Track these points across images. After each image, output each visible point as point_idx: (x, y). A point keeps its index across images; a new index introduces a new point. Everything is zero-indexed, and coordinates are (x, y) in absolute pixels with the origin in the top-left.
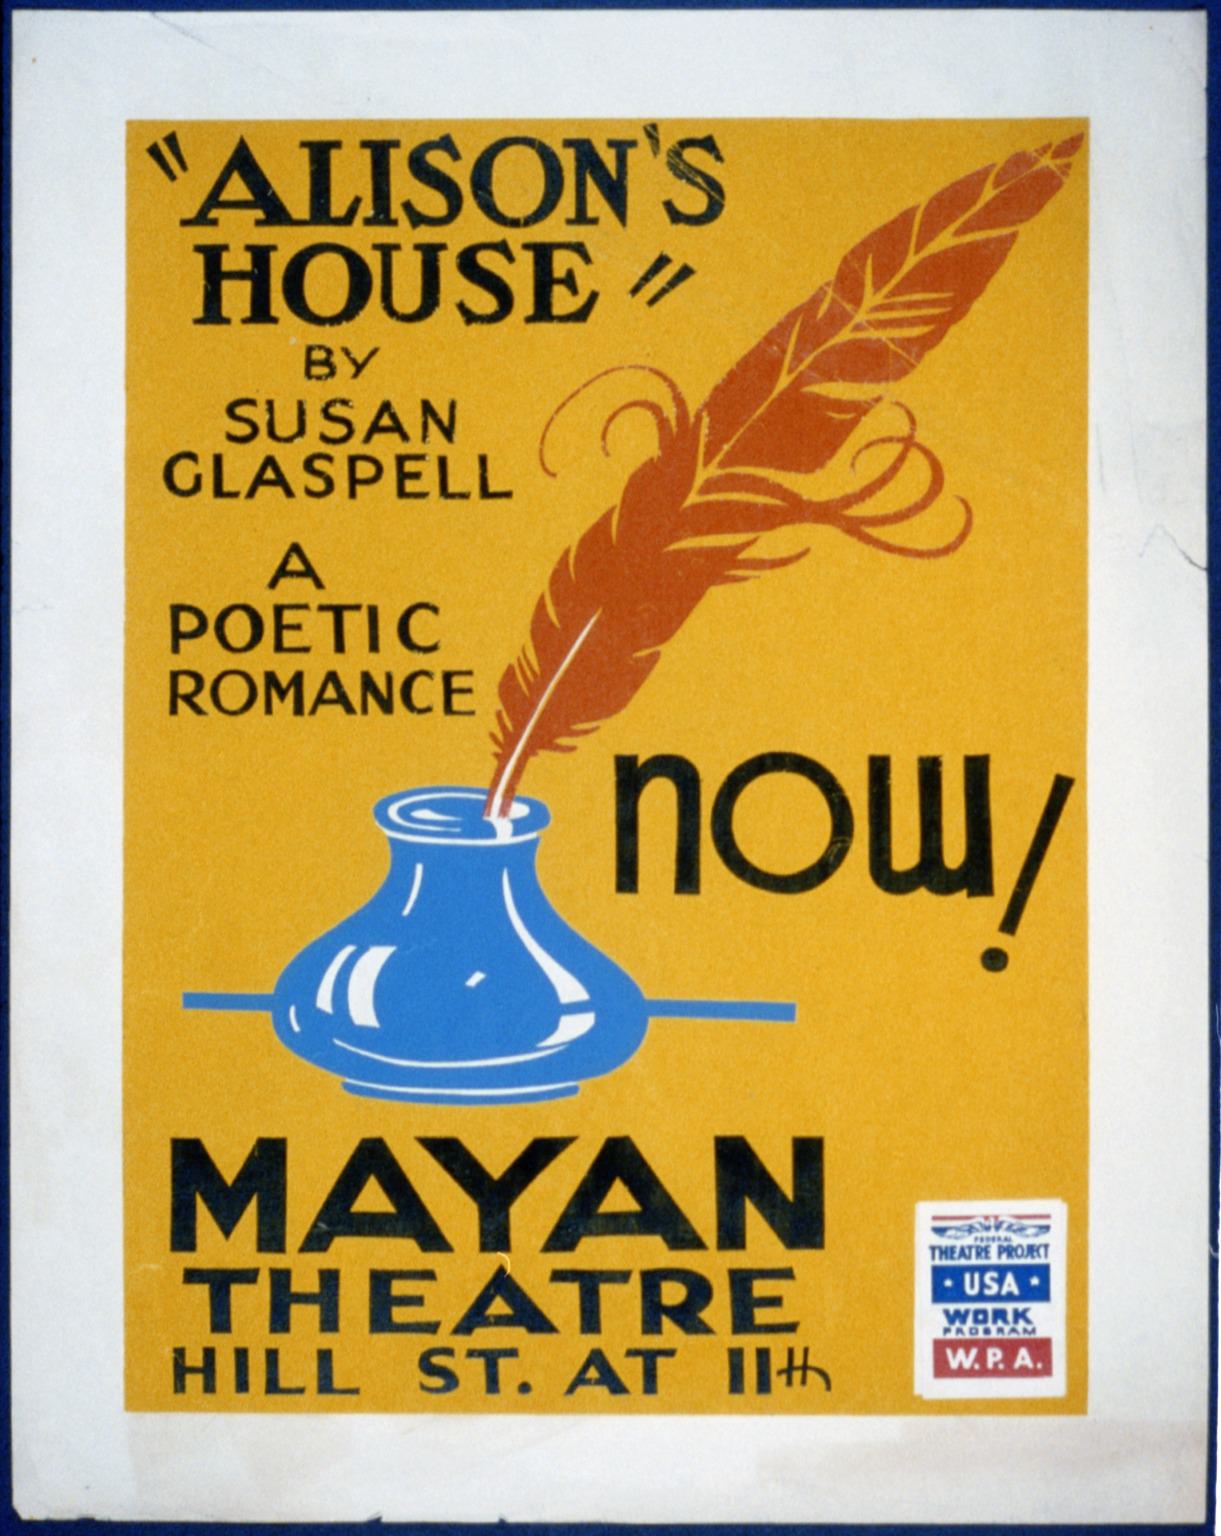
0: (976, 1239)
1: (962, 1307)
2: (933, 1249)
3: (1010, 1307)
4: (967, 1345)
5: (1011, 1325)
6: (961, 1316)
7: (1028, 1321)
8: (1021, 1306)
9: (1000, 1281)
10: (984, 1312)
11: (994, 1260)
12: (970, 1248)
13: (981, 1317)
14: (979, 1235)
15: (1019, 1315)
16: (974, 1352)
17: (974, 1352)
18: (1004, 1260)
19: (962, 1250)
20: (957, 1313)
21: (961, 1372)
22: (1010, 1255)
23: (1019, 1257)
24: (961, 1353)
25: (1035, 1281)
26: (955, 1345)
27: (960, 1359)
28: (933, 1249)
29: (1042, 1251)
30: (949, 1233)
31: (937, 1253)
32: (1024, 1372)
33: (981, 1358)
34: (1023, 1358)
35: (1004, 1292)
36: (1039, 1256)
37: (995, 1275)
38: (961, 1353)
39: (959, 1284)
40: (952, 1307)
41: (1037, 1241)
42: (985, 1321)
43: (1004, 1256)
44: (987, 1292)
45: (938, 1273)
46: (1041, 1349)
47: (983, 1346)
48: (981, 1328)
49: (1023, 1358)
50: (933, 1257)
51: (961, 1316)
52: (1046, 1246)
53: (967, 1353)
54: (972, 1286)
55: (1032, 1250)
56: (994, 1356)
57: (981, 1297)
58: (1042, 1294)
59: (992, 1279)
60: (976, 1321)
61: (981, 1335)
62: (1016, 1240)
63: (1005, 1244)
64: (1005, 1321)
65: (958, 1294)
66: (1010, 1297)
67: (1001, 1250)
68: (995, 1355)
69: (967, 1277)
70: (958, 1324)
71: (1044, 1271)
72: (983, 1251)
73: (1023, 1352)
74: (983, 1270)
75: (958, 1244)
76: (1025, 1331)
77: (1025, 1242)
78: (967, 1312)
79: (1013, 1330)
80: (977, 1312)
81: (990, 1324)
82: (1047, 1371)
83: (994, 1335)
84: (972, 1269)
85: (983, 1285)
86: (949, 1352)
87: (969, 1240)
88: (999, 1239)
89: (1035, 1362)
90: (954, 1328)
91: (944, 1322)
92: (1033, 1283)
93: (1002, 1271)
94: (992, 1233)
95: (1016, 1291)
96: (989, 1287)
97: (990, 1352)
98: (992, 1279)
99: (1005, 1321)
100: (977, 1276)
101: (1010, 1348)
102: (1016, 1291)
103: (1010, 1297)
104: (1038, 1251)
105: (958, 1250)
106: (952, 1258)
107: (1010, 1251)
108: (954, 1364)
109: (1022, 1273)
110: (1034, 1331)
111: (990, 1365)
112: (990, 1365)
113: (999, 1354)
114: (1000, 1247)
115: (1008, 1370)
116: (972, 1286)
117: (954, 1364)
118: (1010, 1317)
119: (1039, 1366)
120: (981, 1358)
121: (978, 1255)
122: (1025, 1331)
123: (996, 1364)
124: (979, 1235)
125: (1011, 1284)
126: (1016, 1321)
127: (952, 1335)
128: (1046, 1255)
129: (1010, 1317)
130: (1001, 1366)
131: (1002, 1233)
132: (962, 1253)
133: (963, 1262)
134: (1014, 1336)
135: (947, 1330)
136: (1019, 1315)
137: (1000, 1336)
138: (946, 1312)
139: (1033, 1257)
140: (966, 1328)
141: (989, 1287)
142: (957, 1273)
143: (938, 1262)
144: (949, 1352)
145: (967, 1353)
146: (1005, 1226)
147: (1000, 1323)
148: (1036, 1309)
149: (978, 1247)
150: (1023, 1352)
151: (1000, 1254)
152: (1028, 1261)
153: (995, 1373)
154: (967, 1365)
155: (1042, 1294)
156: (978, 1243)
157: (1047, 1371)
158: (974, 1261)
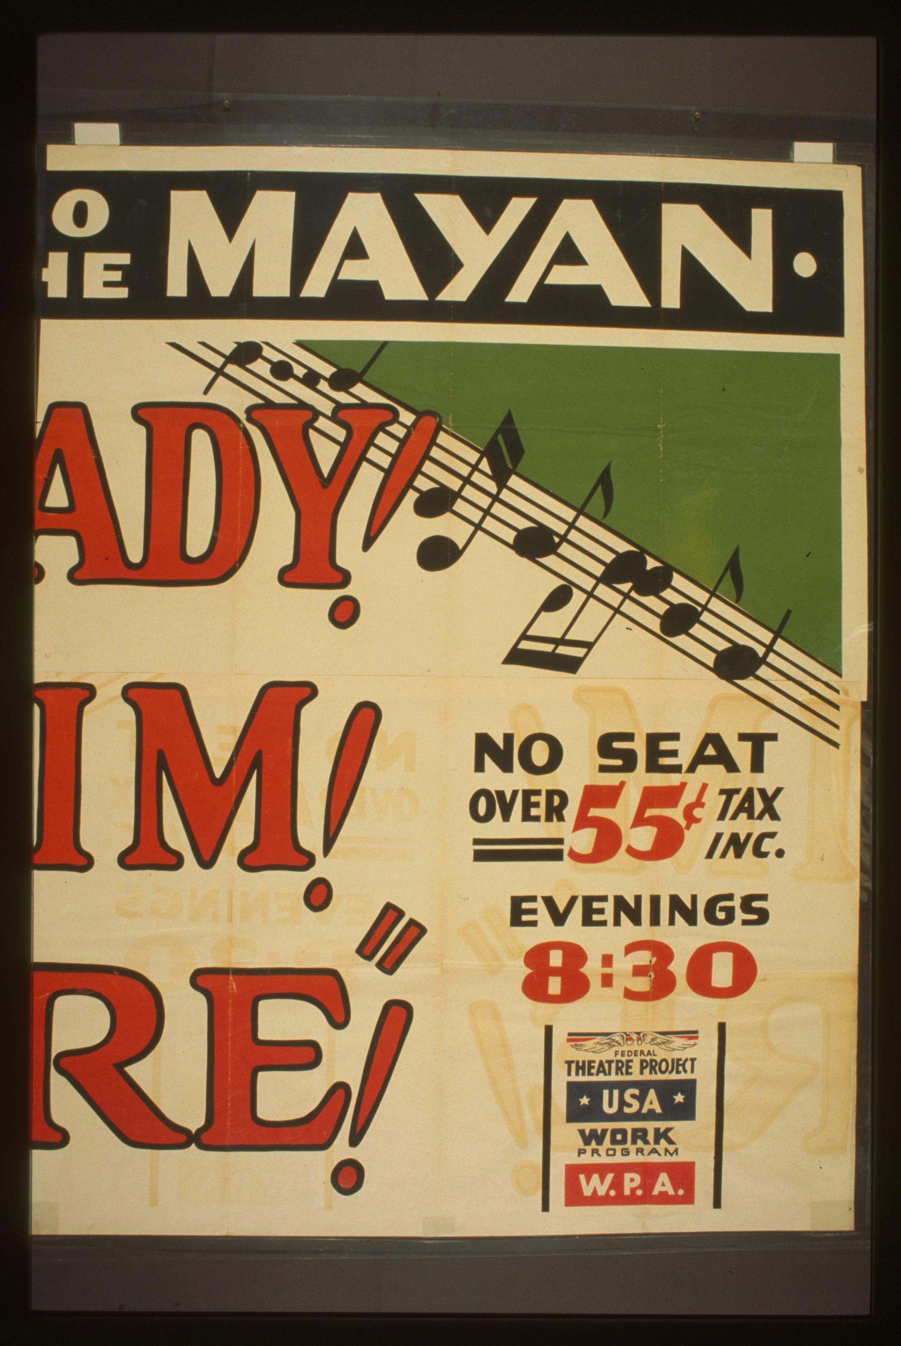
0: (616, 1053)
1: (599, 1126)
2: (569, 1063)
3: (650, 1126)
4: (602, 1170)
5: (652, 1146)
6: (598, 1137)
7: (671, 1142)
8: (662, 1125)
9: (641, 1099)
10: (624, 1132)
11: (636, 1076)
12: (610, 1062)
13: (619, 1137)
14: (620, 1049)
15: (660, 1135)
16: (610, 1177)
17: (610, 1177)
18: (647, 1076)
19: (601, 1064)
20: (593, 1132)
21: (595, 1200)
22: (653, 1070)
23: (662, 1072)
24: (595, 1177)
25: (679, 1098)
26: (589, 1170)
27: (593, 1185)
28: (569, 1063)
29: (688, 1065)
30: (589, 1044)
31: (573, 1066)
32: (664, 1199)
33: (617, 1184)
34: (663, 1184)
35: (644, 1110)
36: (685, 1071)
37: (636, 1092)
38: (595, 1177)
39: (597, 1100)
40: (588, 1127)
41: (683, 1055)
42: (624, 1141)
43: (647, 1071)
44: (627, 1110)
45: (574, 1090)
46: (683, 1175)
47: (619, 1170)
48: (618, 1148)
49: (663, 1184)
50: (569, 1074)
51: (598, 1137)
52: (693, 1060)
53: (602, 1179)
54: (611, 1105)
55: (678, 1065)
56: (632, 1181)
57: (620, 1116)
58: (687, 1112)
59: (633, 1096)
60: (614, 1141)
61: (619, 1159)
62: (660, 1054)
63: (648, 1058)
64: (646, 1142)
65: (594, 1112)
66: (651, 1116)
67: (643, 1066)
68: (632, 1180)
69: (606, 1093)
70: (593, 1144)
71: (689, 1088)
72: (623, 1067)
73: (664, 1177)
74: (623, 1086)
75: (597, 1058)
76: (666, 1150)
77: (670, 1056)
78: (604, 1131)
79: (654, 1151)
80: (614, 1132)
81: (629, 1145)
82: (688, 1198)
83: (633, 1158)
84: (611, 1086)
85: (622, 1103)
86: (582, 1178)
87: (609, 1055)
88: (642, 1052)
89: (676, 1190)
90: (589, 1149)
91: (580, 1143)
92: (677, 1099)
93: (644, 1087)
94: (635, 1046)
95: (658, 1110)
96: (630, 1105)
97: (627, 1176)
98: (633, 1096)
99: (646, 1142)
100: (616, 1093)
101: (649, 1172)
102: (658, 1110)
103: (651, 1116)
104: (683, 1065)
105: (596, 1065)
106: (590, 1074)
107: (653, 1066)
108: (587, 1191)
109: (665, 1090)
110: (676, 1150)
111: (627, 1192)
112: (627, 1192)
113: (638, 1178)
114: (642, 1061)
115: (646, 1197)
116: (611, 1105)
117: (587, 1191)
118: (651, 1137)
119: (681, 1192)
120: (617, 1184)
121: (619, 1070)
122: (666, 1150)
123: (633, 1190)
124: (620, 1049)
125: (653, 1102)
126: (657, 1142)
127: (587, 1159)
128: (692, 1071)
129: (651, 1137)
130: (639, 1192)
131: (646, 1047)
132: (601, 1069)
133: (602, 1078)
134: (654, 1158)
135: (581, 1152)
136: (660, 1135)
137: (640, 1159)
138: (582, 1132)
139: (678, 1072)
140: (602, 1149)
141: (630, 1105)
142: (594, 1090)
143: (574, 1078)
144: (582, 1178)
145: (602, 1179)
146: (648, 1038)
147: (640, 1143)
148: (679, 1128)
149: (618, 1061)
150: (664, 1177)
151: (642, 1073)
152: (674, 1076)
153: (633, 1200)
154: (601, 1192)
155: (687, 1112)
156: (619, 1057)
157: (688, 1198)
158: (613, 1077)
